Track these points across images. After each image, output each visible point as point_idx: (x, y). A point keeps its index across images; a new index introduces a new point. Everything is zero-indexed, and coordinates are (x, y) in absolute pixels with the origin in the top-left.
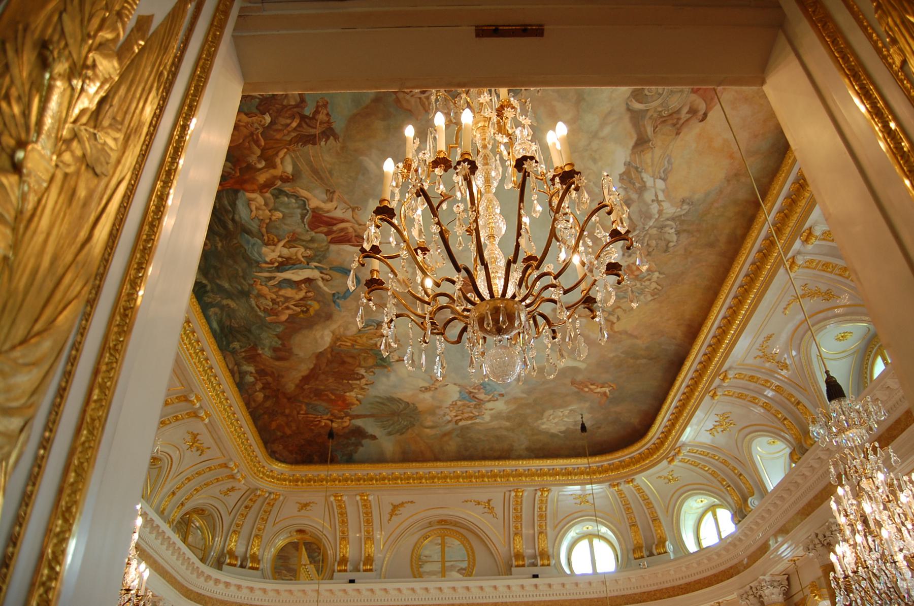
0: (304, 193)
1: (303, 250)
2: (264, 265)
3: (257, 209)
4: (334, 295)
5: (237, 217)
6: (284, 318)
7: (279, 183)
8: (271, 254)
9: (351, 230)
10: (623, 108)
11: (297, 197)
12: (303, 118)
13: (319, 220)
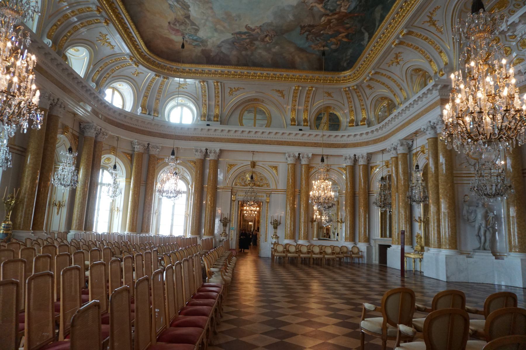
0: (322, 10)
3: (346, 6)
5: (358, 3)
7: (330, 14)
11: (326, 9)
12: (310, 31)
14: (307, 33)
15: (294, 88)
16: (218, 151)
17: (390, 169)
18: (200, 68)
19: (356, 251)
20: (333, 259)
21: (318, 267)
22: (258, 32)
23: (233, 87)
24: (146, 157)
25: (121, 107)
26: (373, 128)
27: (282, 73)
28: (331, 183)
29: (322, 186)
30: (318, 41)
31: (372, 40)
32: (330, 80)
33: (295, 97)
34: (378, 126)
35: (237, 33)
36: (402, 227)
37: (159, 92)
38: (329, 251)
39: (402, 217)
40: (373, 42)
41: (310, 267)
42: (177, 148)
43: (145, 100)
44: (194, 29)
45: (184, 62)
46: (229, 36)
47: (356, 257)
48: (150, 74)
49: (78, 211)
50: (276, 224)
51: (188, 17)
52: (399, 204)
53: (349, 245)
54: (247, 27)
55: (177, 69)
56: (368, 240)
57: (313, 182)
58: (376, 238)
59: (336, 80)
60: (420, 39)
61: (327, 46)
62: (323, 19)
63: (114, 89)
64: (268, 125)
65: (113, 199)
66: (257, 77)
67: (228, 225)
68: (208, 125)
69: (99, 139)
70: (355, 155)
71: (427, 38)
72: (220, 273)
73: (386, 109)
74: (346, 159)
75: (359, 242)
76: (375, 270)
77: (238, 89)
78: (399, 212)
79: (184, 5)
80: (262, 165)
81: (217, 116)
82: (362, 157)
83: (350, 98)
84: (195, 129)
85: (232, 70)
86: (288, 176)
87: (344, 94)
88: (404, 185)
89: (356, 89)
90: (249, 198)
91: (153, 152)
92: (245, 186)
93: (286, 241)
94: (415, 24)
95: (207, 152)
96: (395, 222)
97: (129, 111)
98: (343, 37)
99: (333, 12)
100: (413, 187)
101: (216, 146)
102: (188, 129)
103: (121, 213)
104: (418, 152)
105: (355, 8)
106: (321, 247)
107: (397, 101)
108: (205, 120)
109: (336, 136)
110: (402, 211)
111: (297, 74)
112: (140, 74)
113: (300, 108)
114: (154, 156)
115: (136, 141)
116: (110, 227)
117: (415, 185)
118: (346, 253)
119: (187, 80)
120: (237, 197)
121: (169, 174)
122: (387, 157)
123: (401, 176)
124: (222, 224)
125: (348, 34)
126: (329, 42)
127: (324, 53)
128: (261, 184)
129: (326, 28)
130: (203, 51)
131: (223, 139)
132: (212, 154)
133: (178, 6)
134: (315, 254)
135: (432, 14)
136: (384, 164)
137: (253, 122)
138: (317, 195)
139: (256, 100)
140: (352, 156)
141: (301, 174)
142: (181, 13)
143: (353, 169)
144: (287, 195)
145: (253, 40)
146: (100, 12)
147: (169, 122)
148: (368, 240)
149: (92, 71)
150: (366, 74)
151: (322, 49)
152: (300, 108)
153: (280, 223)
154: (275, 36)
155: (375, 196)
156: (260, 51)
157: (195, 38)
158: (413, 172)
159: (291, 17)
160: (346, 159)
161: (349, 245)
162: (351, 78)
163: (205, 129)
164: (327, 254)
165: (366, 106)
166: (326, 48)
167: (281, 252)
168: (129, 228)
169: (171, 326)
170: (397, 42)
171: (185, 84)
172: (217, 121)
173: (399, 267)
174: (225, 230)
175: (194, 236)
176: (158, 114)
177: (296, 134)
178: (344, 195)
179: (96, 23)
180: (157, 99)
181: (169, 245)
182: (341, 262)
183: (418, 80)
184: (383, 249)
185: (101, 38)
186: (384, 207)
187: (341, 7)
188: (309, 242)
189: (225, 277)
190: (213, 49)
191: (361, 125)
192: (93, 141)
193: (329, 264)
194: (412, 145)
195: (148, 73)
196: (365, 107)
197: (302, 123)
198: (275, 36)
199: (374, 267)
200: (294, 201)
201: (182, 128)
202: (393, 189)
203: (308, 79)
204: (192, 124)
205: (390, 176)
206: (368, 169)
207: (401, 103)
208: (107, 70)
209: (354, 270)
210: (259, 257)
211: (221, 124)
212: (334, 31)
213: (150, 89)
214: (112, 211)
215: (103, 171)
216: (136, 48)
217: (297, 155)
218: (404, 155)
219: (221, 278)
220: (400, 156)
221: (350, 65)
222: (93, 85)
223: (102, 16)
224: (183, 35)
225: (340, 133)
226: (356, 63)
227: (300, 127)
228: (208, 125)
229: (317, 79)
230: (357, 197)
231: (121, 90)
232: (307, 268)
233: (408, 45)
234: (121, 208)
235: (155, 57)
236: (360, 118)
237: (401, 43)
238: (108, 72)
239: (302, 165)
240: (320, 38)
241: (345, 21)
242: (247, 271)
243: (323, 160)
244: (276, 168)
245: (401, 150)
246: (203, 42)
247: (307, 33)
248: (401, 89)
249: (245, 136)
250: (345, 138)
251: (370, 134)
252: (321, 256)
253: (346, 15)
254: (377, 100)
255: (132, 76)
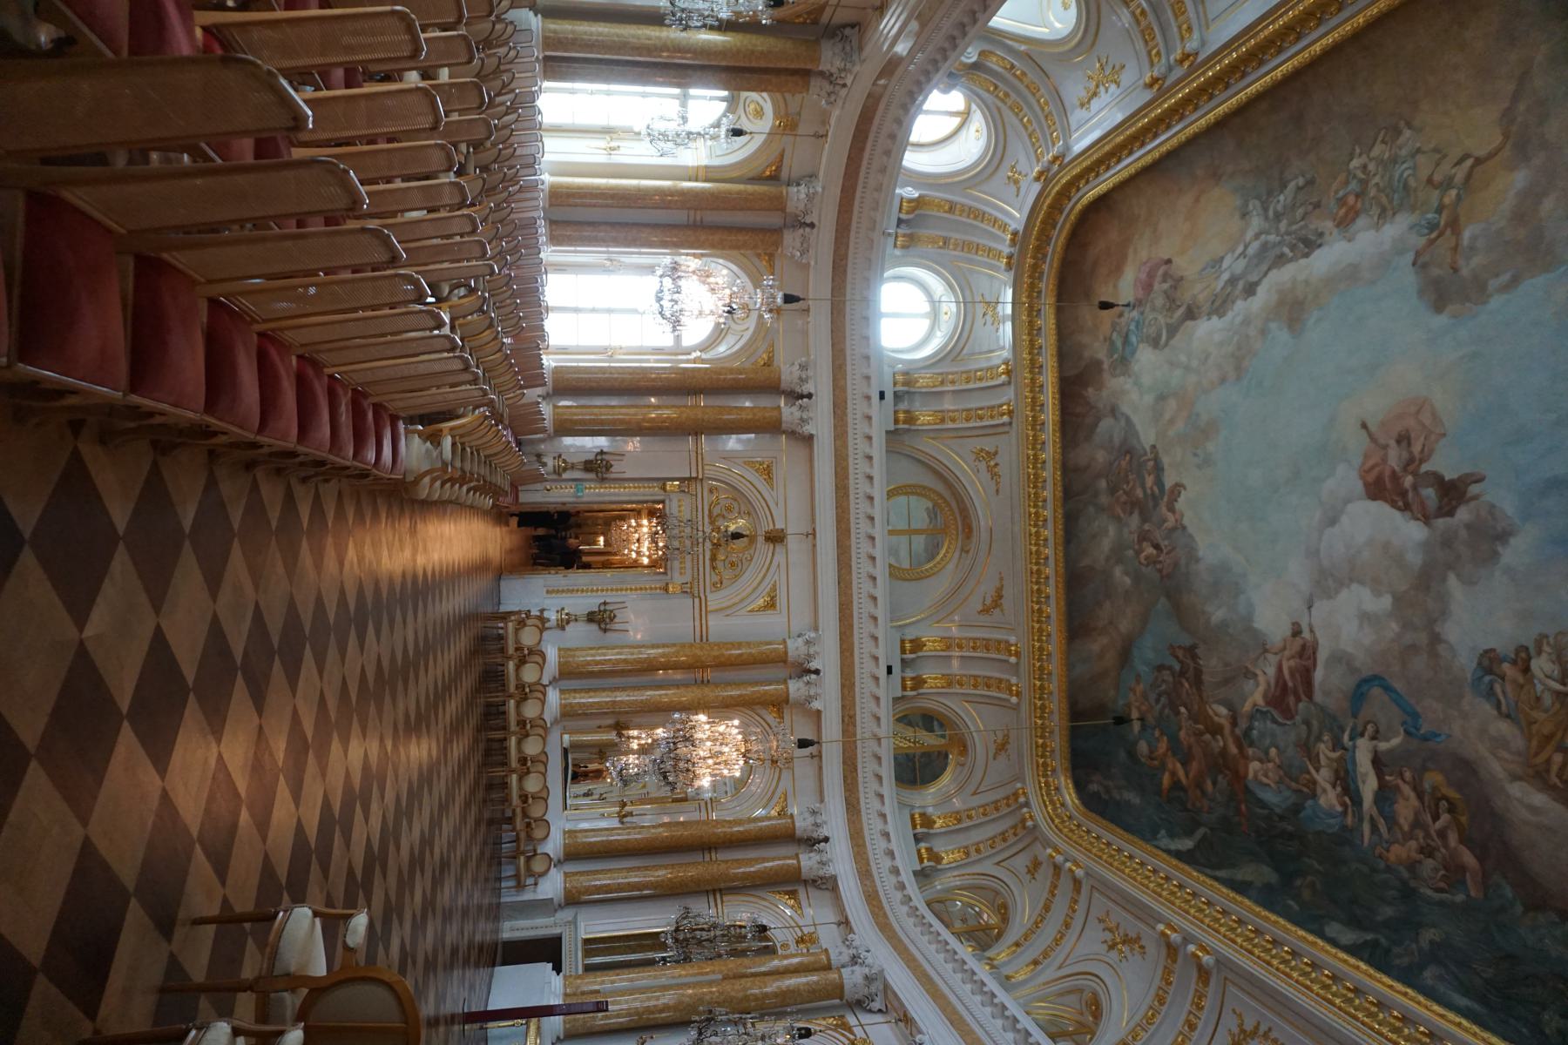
0: (1247, 707)
1: (1322, 746)
2: (1349, 820)
3: (1266, 776)
4: (1407, 732)
5: (1278, 810)
6: (1469, 859)
7: (1238, 731)
8: (1329, 798)
9: (1292, 663)
10: (1167, 350)
11: (1252, 717)
12: (1182, 673)
13: (1282, 698)
14: (1177, 667)
15: (1013, 639)
16: (809, 429)
17: (793, 949)
18: (1048, 360)
19: (538, 866)
20: (506, 800)
21: (478, 757)
22: (1165, 521)
23: (998, 459)
24: (774, 220)
25: (913, 138)
26: (912, 888)
27: (1053, 601)
28: (738, 774)
29: (726, 749)
30: (1158, 701)
31: (1174, 862)
32: (1044, 746)
33: (987, 645)
34: (919, 901)
35: (1157, 460)
36: (618, 1003)
37: (966, 246)
38: (532, 785)
39: (649, 999)
40: (1167, 865)
41: (479, 730)
42: (808, 310)
43: (939, 206)
44: (1159, 336)
45: (1059, 311)
46: (1147, 436)
47: (518, 869)
48: (1016, 216)
49: (600, 34)
50: (601, 619)
51: (1191, 315)
52: (688, 985)
53: (553, 845)
54: (1178, 488)
55: (1040, 292)
56: (573, 900)
57: (736, 722)
58: (582, 926)
59: (1045, 765)
60: (1188, 1006)
61: (1144, 728)
62: (1223, 711)
63: (966, 116)
64: (895, 573)
65: (644, 132)
66: (1033, 530)
67: (592, 476)
68: (882, 395)
69: (815, 83)
70: (826, 840)
71: (1192, 1027)
72: (439, 465)
73: (972, 922)
74: (814, 813)
75: (566, 874)
76: (482, 932)
77: (994, 474)
78: (665, 988)
79: (1224, 302)
80: (775, 563)
81: (911, 419)
82: (822, 863)
83: (997, 809)
84: (867, 358)
85: (1050, 454)
86: (748, 644)
87: (1008, 790)
88: (746, 998)
89: (1024, 827)
90: (676, 531)
91: (791, 239)
92: (710, 516)
93: (552, 654)
94: (1232, 989)
95: (802, 397)
96: (631, 980)
97: (905, 163)
98: (1173, 774)
99: (1245, 740)
100: (745, 1025)
101: (820, 423)
102: (867, 338)
103: (602, 158)
104: (850, 1030)
105: (1262, 804)
106: (542, 760)
107: (1001, 953)
108: (895, 384)
109: (879, 778)
110: (668, 998)
111: (1055, 646)
112: (1013, 188)
113: (955, 663)
114: (778, 244)
115: (820, 189)
116: (558, 130)
117: (751, 1030)
118: (530, 838)
119: (1009, 326)
120: (675, 498)
121: (728, 292)
122: (829, 937)
123: (773, 986)
124: (592, 457)
125: (1184, 790)
126: (1157, 733)
127: (1122, 720)
128: (719, 565)
129: (1196, 722)
130: (1097, 364)
131: (845, 445)
132: (797, 414)
133: (1221, 283)
134: (519, 743)
135: (1266, 1035)
136: (806, 930)
137: (903, 526)
138: (699, 735)
139: (968, 530)
140: (824, 832)
141: (756, 683)
142: (1197, 291)
143: (785, 836)
144: (691, 646)
145: (1144, 508)
146: (1181, 62)
147: (882, 281)
148: (573, 900)
149: (1011, 50)
150: (1075, 854)
151: (1135, 714)
152: (955, 663)
153: (605, 631)
154: (1160, 571)
155: (706, 911)
156: (1112, 530)
157: (1134, 339)
158: (787, 1022)
159: (1218, 615)
160: (814, 813)
161: (553, 845)
162: (1055, 809)
163: (869, 385)
164: (520, 779)
165: (974, 863)
166: (1136, 726)
167: (517, 641)
168: (561, 186)
169: (261, 335)
170: (1174, 937)
171: (997, 321)
172: (896, 421)
173: (497, 1002)
174: (573, 467)
175: (548, 378)
176: (903, 247)
177: (876, 659)
178: (704, 817)
179: (1149, 53)
180: (946, 241)
181: (520, 306)
182: (499, 825)
183: (1068, 1011)
184: (547, 951)
185: (1108, 70)
186: (677, 940)
187: (1261, 761)
188: (555, 722)
189: (427, 480)
190: (1104, 393)
191: (919, 851)
192: (809, 67)
193: (490, 787)
194: (870, 1011)
195: (1019, 210)
196: (974, 856)
197: (909, 674)
198: (1160, 571)
199: (490, 926)
200: (676, 667)
201: (866, 319)
202: (733, 964)
203: (1040, 679)
204: (880, 350)
205: (770, 951)
206: (789, 883)
207: (993, 967)
208: (1019, 93)
209: (478, 867)
210: (499, 577)
211: (887, 432)
212: (1190, 747)
213: (975, 218)
214: (607, 131)
215: (723, 99)
216: (1089, 170)
217: (814, 665)
218: (838, 990)
219: (425, 467)
220: (833, 976)
221: (1095, 804)
222: (971, 55)
223: (1170, 69)
224: (1138, 304)
225: (889, 787)
226: (1098, 818)
227: (896, 669)
228: (882, 395)
229: (1043, 707)
230: (703, 856)
231: (964, 132)
232: (473, 722)
233: (1168, 971)
234: (618, 159)
235: (1068, 226)
236: (939, 846)
237: (1172, 950)
238: (1013, 95)
239: (785, 682)
240: (1164, 707)
241: (1220, 778)
242: (455, 541)
243: (803, 744)
244: (771, 605)
245: (852, 978)
246: (1123, 363)
247: (1177, 667)
248: (1036, 963)
249: (858, 508)
250: (876, 804)
251: (893, 880)
252: (514, 764)
253: (1238, 777)
254: (997, 893)
255: (1007, 164)
